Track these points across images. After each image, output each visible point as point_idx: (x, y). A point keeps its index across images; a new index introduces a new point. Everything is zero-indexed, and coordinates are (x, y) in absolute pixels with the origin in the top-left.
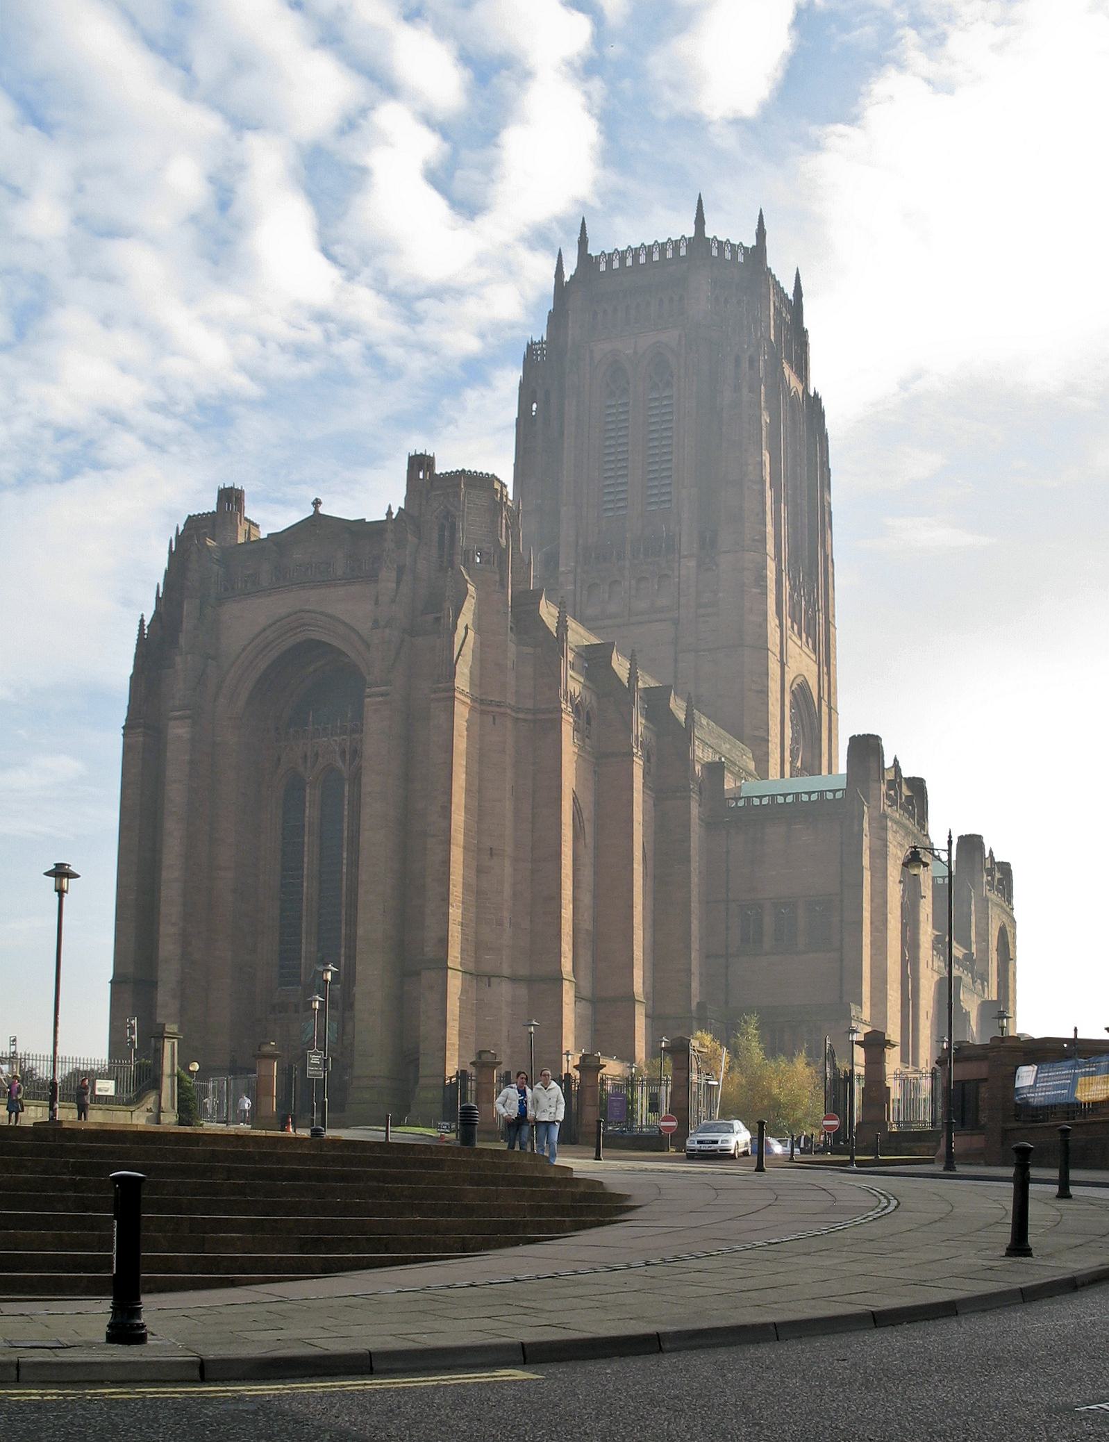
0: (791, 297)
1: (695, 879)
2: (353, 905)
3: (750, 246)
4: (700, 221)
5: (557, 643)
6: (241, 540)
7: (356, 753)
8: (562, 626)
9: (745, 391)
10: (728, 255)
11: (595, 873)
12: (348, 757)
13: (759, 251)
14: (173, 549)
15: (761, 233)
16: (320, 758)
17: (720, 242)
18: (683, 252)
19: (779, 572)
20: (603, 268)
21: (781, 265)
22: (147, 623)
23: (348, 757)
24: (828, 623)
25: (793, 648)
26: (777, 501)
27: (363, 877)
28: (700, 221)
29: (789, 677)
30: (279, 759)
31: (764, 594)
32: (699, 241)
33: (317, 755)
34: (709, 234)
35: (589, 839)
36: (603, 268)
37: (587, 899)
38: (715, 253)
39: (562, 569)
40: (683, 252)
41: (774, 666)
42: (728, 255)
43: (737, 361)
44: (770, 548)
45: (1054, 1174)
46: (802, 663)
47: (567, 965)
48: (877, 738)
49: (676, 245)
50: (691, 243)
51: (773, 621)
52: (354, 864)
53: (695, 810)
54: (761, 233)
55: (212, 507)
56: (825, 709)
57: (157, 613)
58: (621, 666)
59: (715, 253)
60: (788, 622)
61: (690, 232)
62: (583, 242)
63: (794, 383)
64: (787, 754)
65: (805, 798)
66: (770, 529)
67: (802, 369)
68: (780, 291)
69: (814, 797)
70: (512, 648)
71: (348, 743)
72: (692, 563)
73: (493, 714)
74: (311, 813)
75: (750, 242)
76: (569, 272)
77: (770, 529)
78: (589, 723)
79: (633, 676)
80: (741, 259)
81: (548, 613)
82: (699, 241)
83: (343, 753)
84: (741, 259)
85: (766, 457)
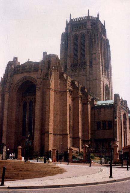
0: (103, 24)
1: (89, 118)
2: (34, 123)
5: (66, 81)
6: (17, 65)
7: (35, 98)
8: (67, 78)
9: (96, 39)
10: (93, 19)
11: (73, 117)
12: (33, 99)
13: (98, 18)
15: (98, 15)
17: (92, 17)
18: (86, 18)
19: (102, 68)
21: (102, 20)
22: (2, 78)
23: (33, 99)
24: (111, 75)
25: (105, 80)
26: (102, 56)
27: (36, 118)
29: (104, 84)
31: (100, 71)
32: (89, 17)
34: (90, 15)
35: (72, 112)
37: (71, 121)
38: (91, 18)
39: (68, 68)
40: (86, 18)
41: (102, 83)
42: (93, 19)
43: (95, 34)
44: (101, 64)
45: (126, 167)
46: (106, 82)
47: (68, 133)
49: (85, 17)
50: (87, 17)
51: (101, 75)
52: (34, 116)
53: (89, 106)
54: (98, 15)
55: (12, 60)
56: (111, 89)
57: (4, 77)
58: (77, 84)
59: (91, 18)
60: (104, 75)
61: (87, 15)
62: (70, 17)
63: (104, 38)
64: (104, 97)
65: (107, 104)
66: (101, 61)
67: (105, 36)
68: (101, 24)
69: (109, 104)
70: (59, 81)
72: (89, 66)
74: (28, 108)
75: (96, 16)
76: (68, 21)
77: (101, 61)
78: (72, 93)
79: (79, 85)
80: (95, 19)
81: (65, 75)
82: (89, 17)
83: (33, 98)
84: (95, 19)
85: (100, 49)
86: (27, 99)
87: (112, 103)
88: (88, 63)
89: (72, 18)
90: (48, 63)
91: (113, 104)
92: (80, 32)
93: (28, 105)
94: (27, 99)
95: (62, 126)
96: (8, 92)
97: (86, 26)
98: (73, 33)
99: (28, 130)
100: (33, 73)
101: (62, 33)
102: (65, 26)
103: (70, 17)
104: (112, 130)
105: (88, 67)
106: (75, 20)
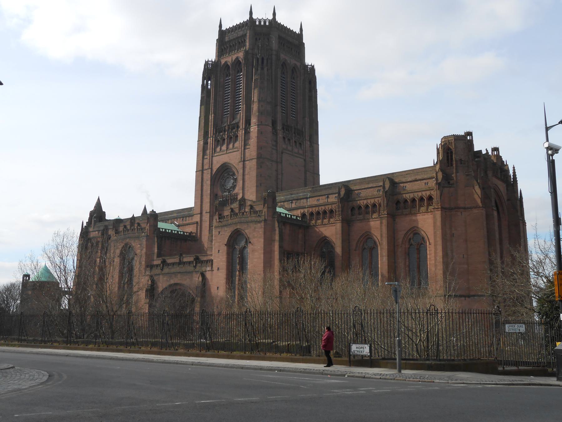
3: (271, 19)
4: (251, 13)
10: (262, 23)
15: (274, 14)
28: (251, 13)
34: (254, 17)
38: (257, 23)
42: (262, 23)
54: (274, 14)
59: (257, 23)
62: (220, 26)
75: (271, 17)
80: (267, 24)
84: (267, 24)
88: (242, 125)
92: (234, 57)
98: (223, 61)
101: (207, 63)
103: (220, 26)
105: (241, 133)
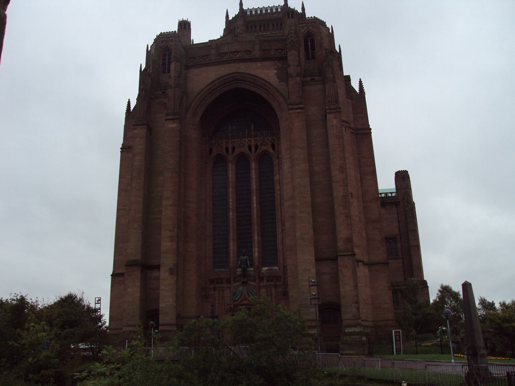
14: (149, 49)
15: (303, 9)
16: (236, 150)
18: (279, 10)
20: (248, 13)
30: (211, 151)
33: (234, 149)
36: (248, 13)
40: (279, 10)
48: (406, 172)
49: (277, 9)
54: (303, 9)
55: (174, 28)
61: (282, 3)
62: (241, 4)
71: (253, 142)
73: (346, 126)
83: (250, 148)
86: (227, 149)
87: (391, 193)
89: (245, 7)
90: (306, 41)
91: (394, 195)
93: (231, 169)
94: (227, 149)
95: (364, 234)
96: (177, 117)
97: (281, 24)
99: (236, 248)
100: (259, 64)
102: (224, 27)
103: (241, 4)
104: (401, 260)
106: (251, 11)
